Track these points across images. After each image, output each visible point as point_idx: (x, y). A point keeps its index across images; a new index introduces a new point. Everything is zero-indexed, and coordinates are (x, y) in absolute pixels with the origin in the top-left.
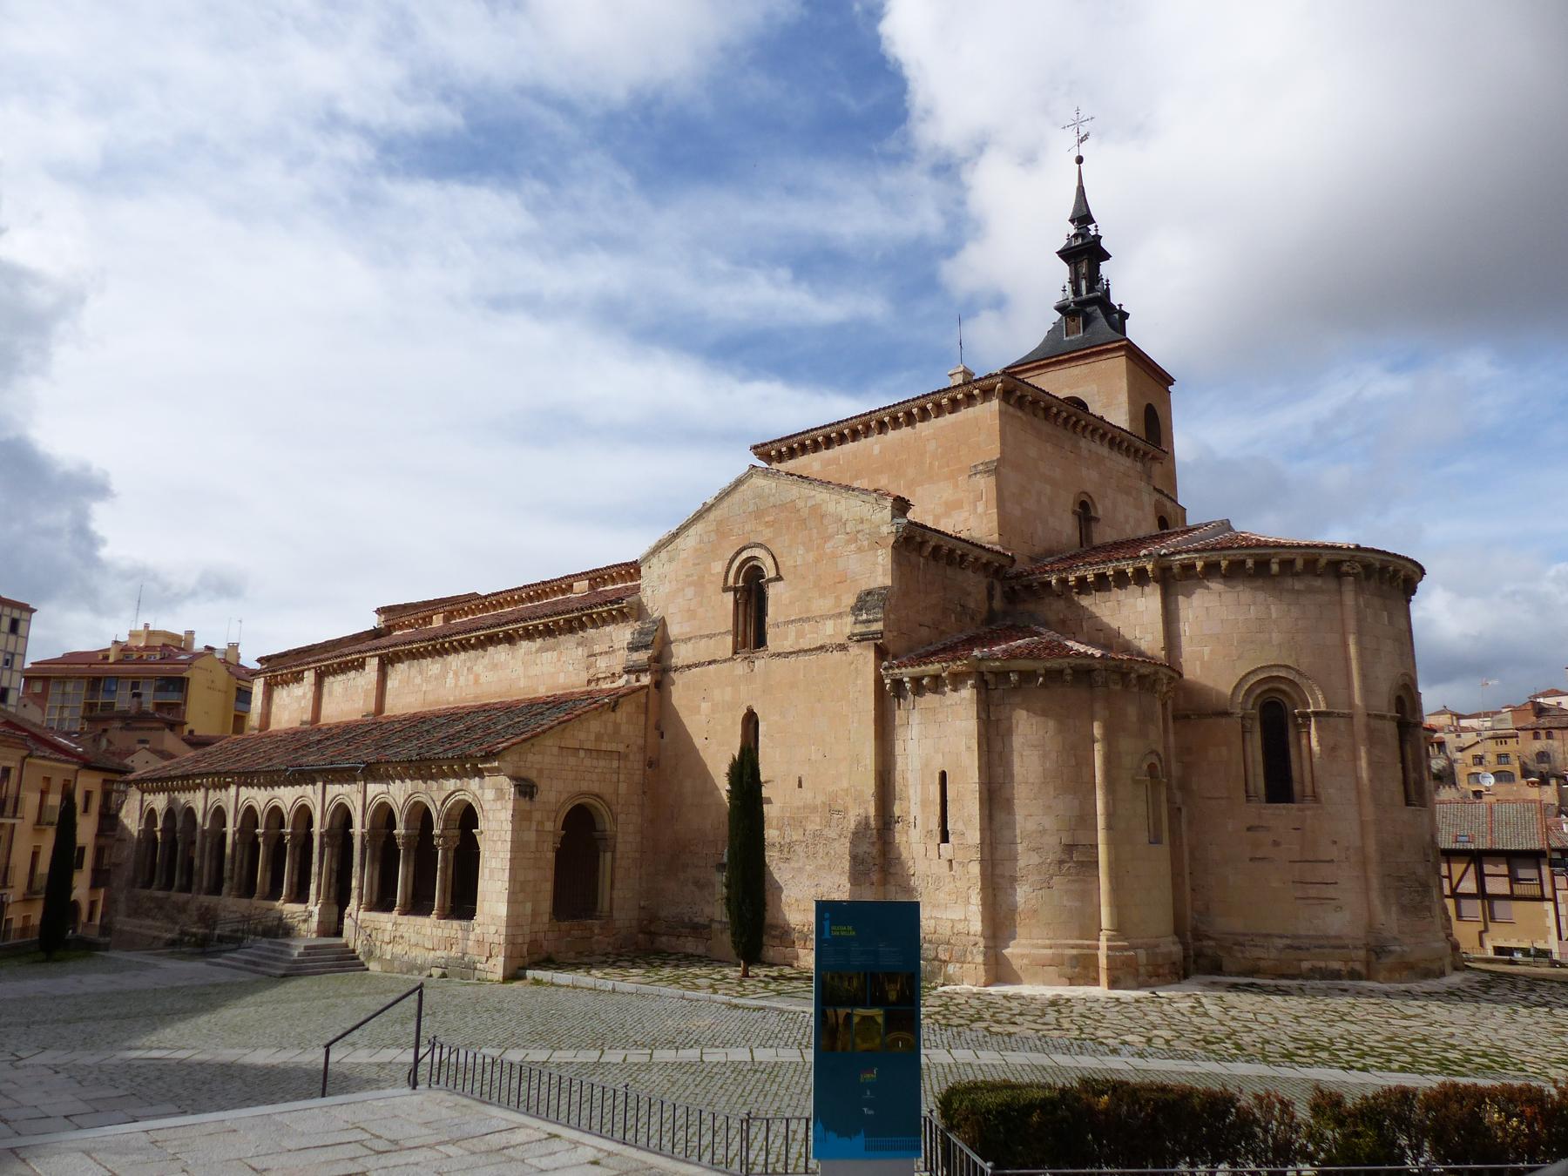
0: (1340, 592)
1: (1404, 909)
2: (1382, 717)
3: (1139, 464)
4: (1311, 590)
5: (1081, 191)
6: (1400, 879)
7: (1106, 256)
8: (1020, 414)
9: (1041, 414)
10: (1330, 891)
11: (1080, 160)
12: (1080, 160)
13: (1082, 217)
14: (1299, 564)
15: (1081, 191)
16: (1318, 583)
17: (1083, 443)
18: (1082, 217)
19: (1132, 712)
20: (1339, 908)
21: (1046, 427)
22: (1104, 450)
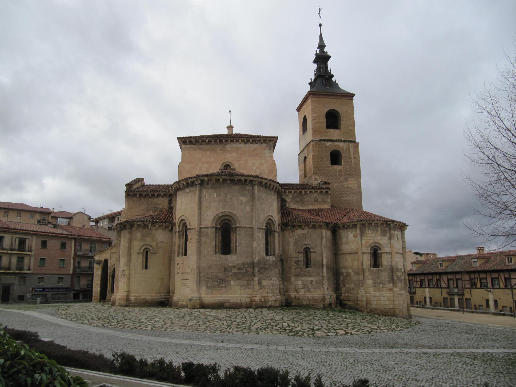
0: (196, 190)
1: (208, 287)
2: (207, 228)
3: (264, 145)
4: (190, 192)
5: (321, 35)
6: (209, 278)
7: (329, 57)
8: (192, 146)
9: (204, 143)
10: (187, 282)
11: (320, 25)
12: (320, 25)
13: (322, 46)
14: (185, 184)
15: (321, 35)
16: (192, 189)
17: (228, 147)
18: (322, 46)
19: (139, 235)
20: (188, 287)
21: (208, 146)
22: (242, 145)
